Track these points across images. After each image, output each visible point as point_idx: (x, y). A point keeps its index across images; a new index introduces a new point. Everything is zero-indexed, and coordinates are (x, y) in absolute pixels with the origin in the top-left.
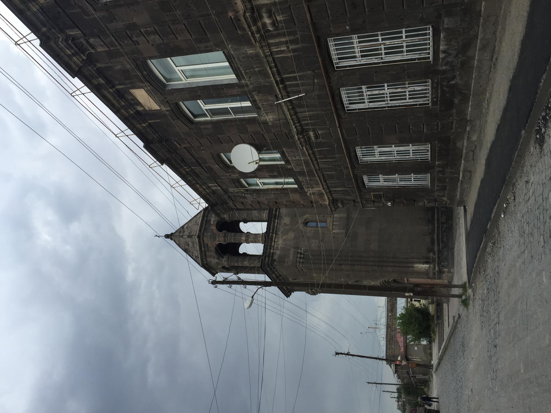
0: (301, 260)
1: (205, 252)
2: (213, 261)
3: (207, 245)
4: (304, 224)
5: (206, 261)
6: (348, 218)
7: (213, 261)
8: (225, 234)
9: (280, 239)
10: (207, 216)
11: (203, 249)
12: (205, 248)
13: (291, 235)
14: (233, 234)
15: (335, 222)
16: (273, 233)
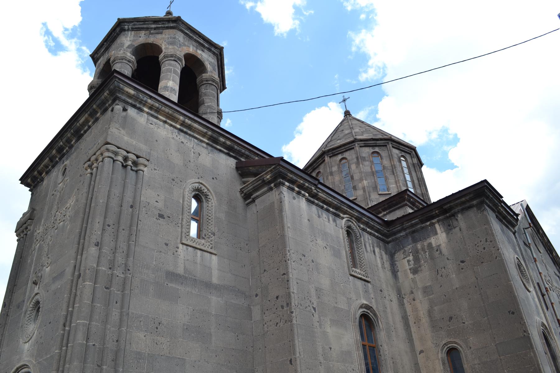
0: (120, 158)
1: (147, 29)
2: (128, 40)
3: (161, 33)
4: (198, 190)
5: (128, 30)
6: (208, 285)
7: (128, 40)
8: (180, 59)
9: (170, 135)
10: (210, 50)
11: (153, 26)
12: (155, 29)
13: (177, 159)
14: (179, 72)
15: (202, 256)
16: (183, 124)
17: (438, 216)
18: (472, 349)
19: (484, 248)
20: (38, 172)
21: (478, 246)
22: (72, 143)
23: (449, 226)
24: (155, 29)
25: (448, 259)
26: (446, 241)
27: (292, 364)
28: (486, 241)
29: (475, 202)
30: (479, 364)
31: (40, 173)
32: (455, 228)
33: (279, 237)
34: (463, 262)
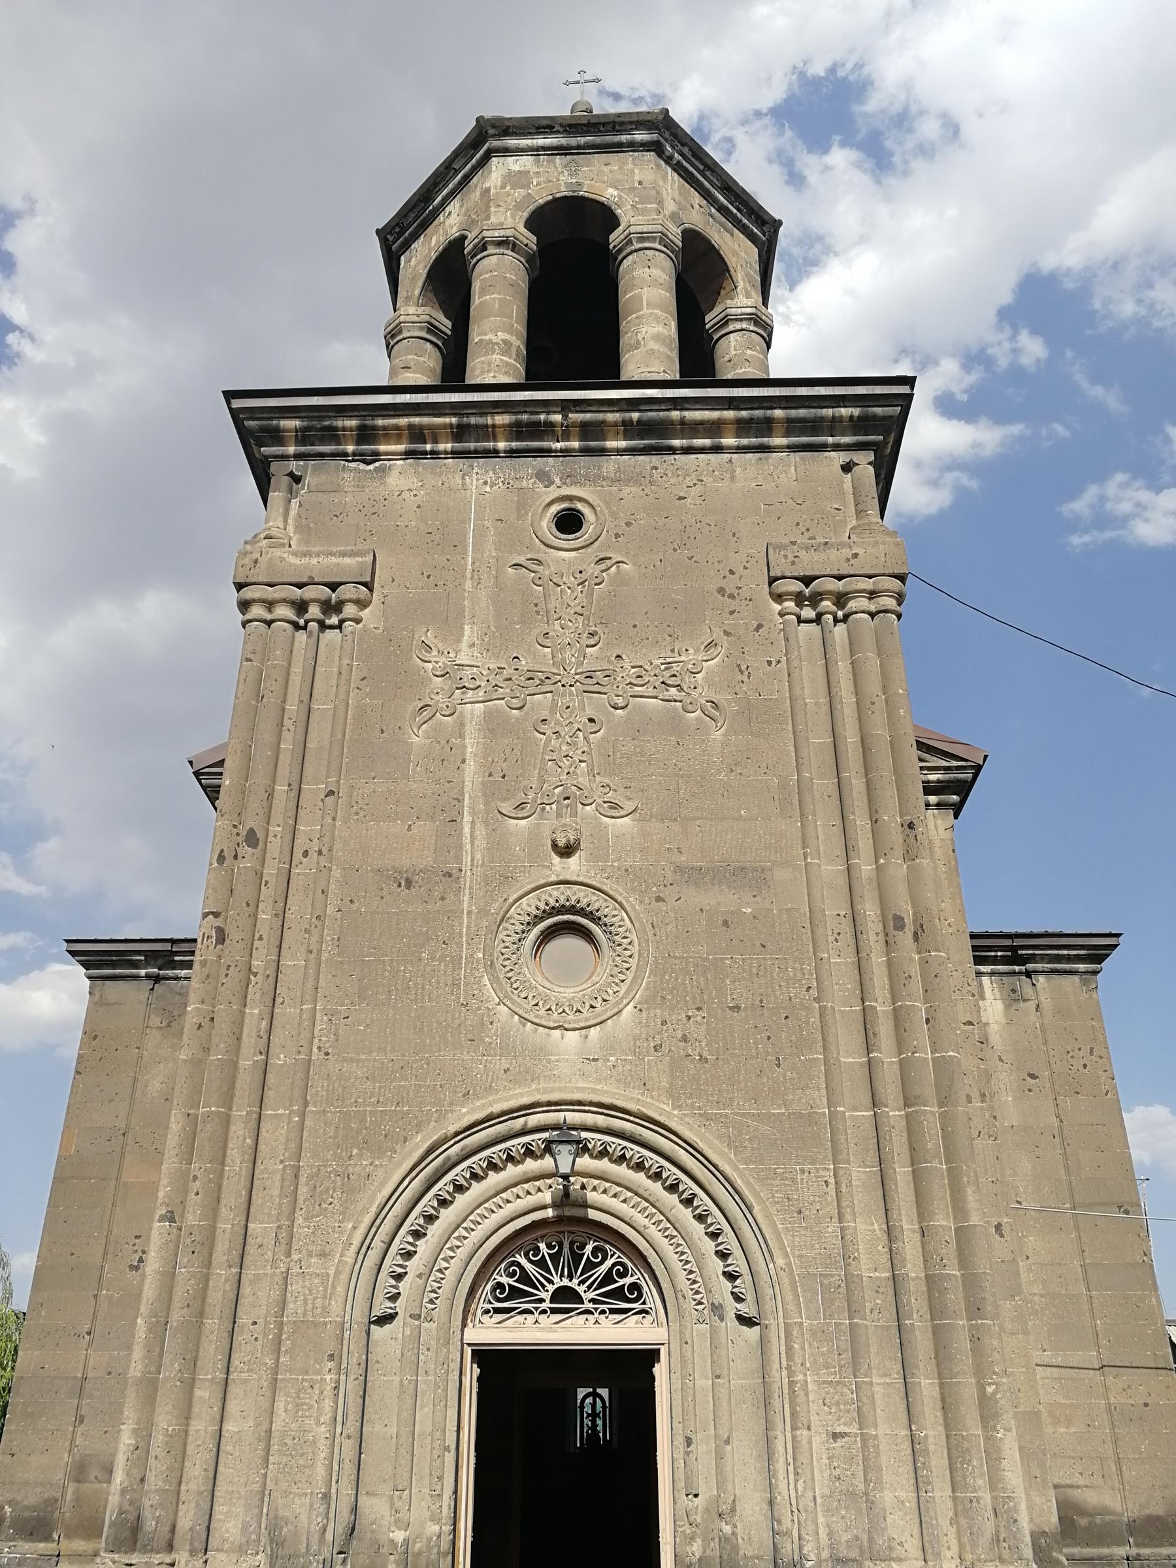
17: (994, 961)
18: (1030, 1261)
19: (1085, 1066)
20: (361, 428)
21: (1072, 1057)
22: (610, 444)
23: (1014, 991)
24: (722, 209)
25: (1001, 1060)
26: (1003, 1021)
27: (1002, 1236)
28: (1091, 1053)
29: (1081, 967)
30: (1042, 1296)
31: (366, 435)
32: (1025, 1000)
33: (950, 930)
34: (1032, 1076)
